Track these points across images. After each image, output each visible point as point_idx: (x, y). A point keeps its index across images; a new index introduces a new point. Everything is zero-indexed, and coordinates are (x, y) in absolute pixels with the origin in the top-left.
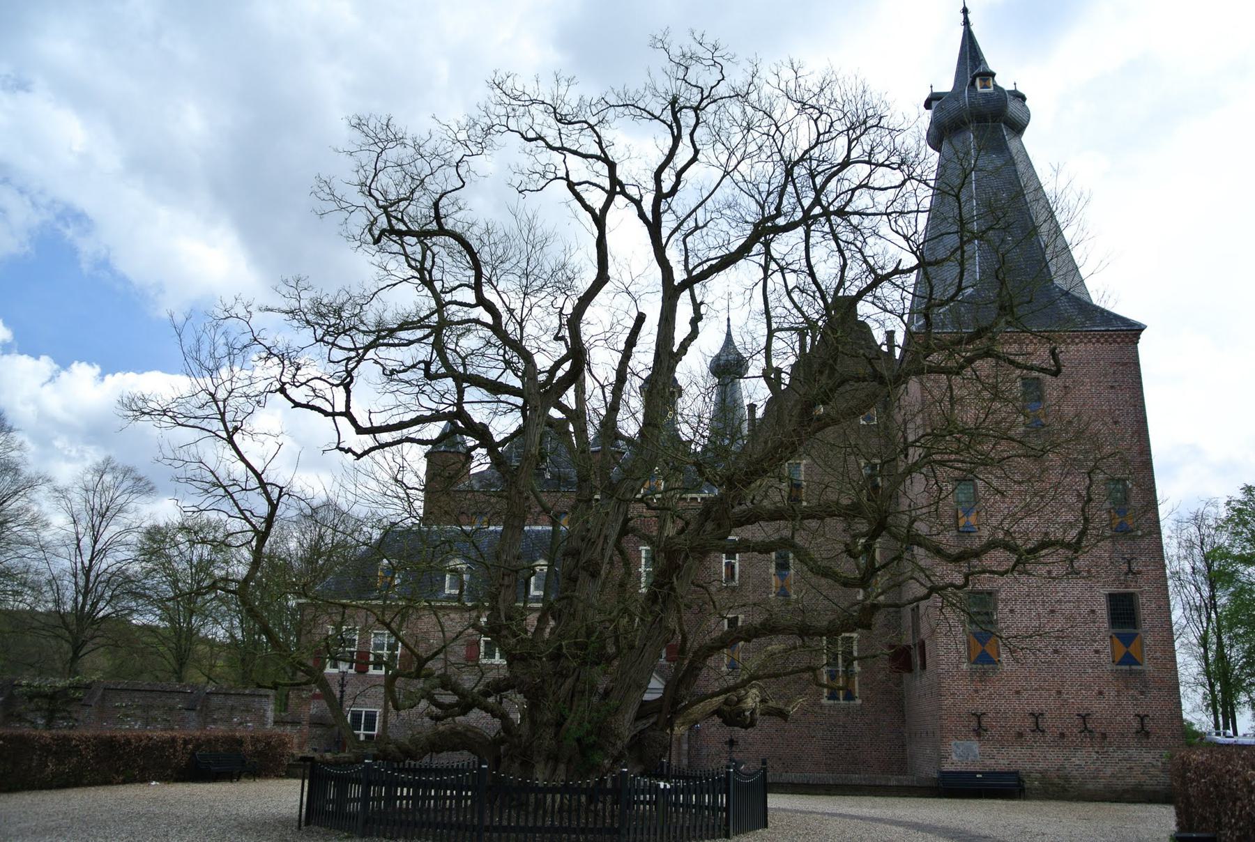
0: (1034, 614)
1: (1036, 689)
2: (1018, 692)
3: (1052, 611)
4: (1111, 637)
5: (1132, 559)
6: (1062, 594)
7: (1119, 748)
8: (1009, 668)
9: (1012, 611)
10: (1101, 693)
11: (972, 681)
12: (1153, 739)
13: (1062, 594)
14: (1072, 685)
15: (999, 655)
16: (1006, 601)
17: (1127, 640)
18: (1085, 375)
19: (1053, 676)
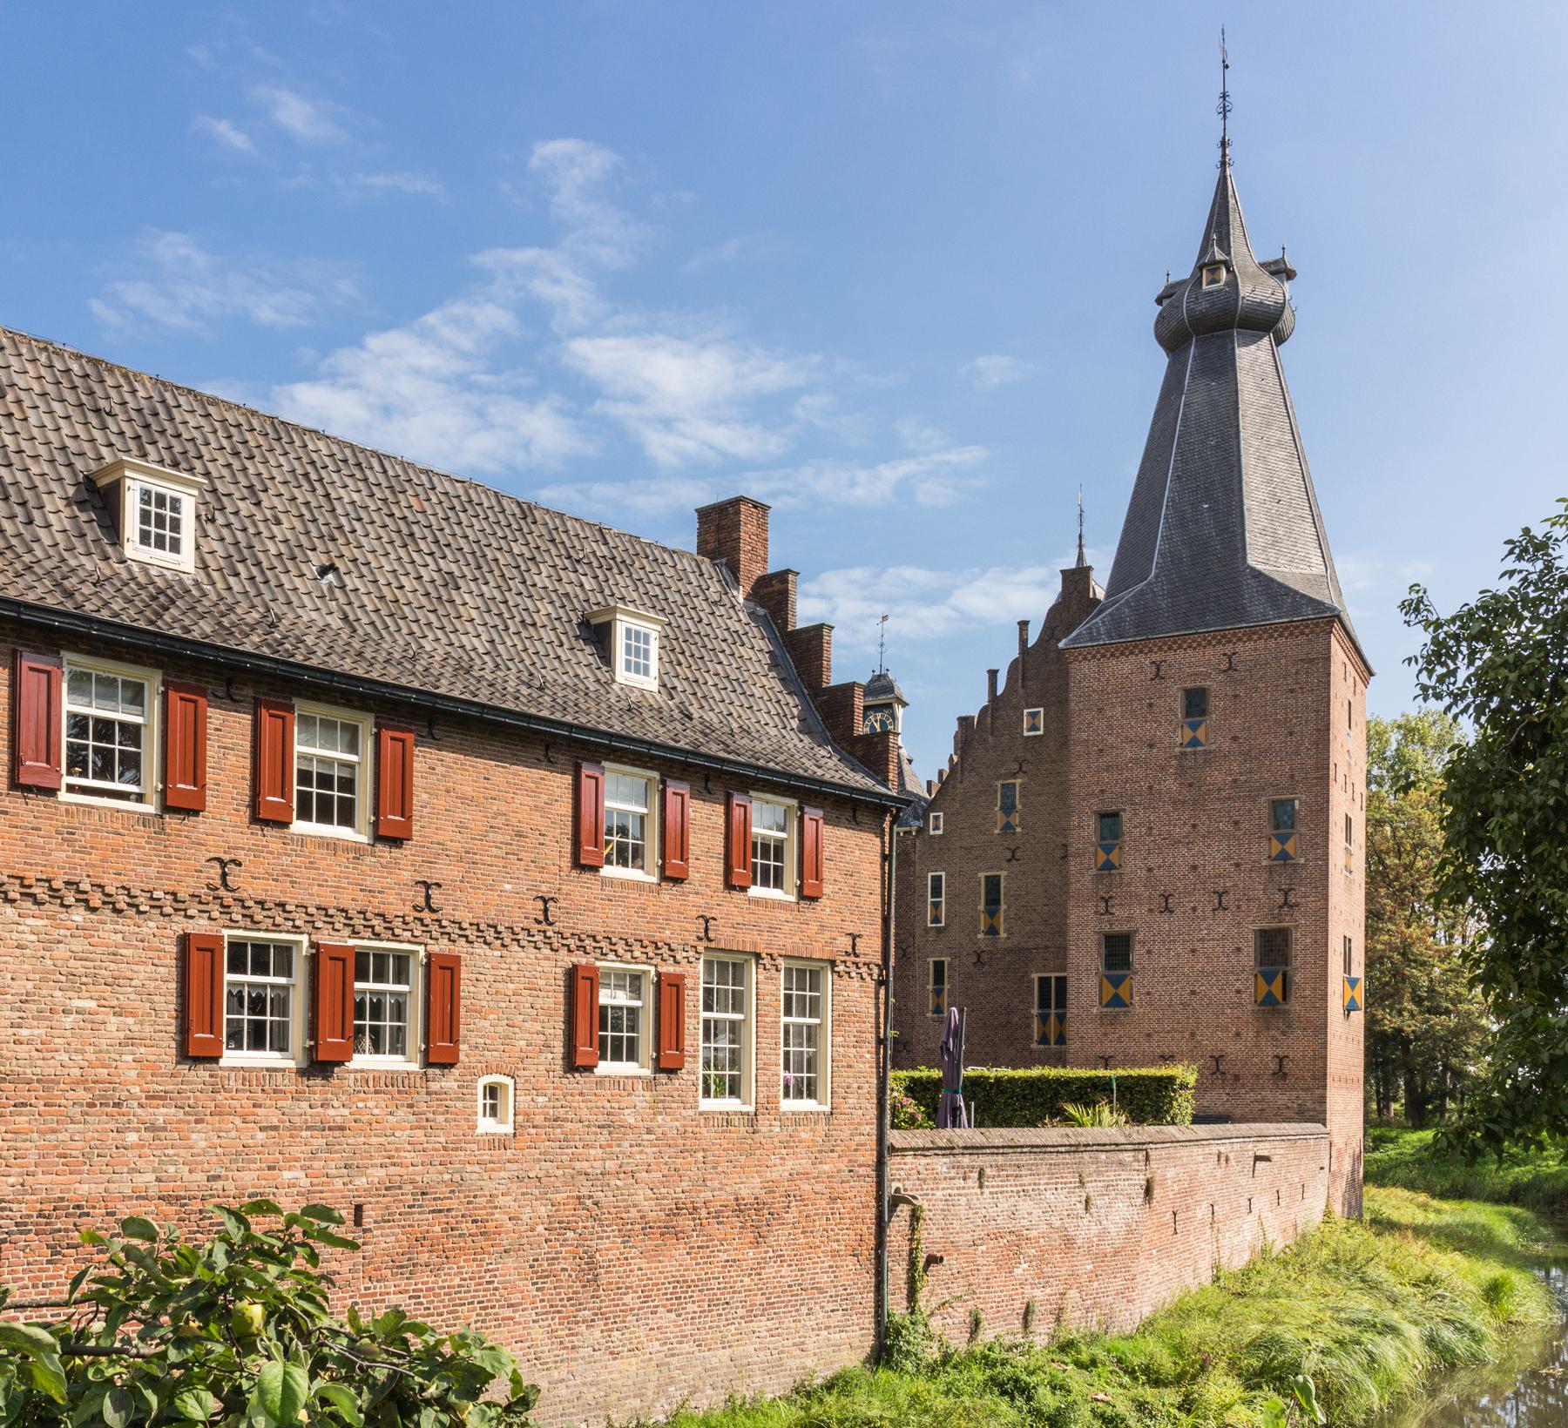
1: (1168, 1032)
2: (1148, 1035)
3: (1193, 951)
7: (1252, 1090)
9: (1149, 952)
10: (1238, 1034)
12: (1290, 1080)
15: (1132, 998)
16: (1143, 943)
17: (1116, 982)
18: (1261, 678)
19: (1188, 1018)
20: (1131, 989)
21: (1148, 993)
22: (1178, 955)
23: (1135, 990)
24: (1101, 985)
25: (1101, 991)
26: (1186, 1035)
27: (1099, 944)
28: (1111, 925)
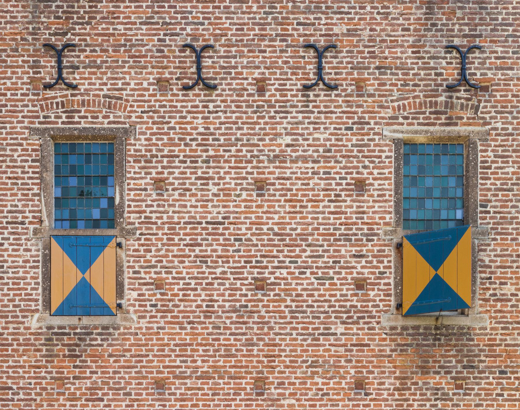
0: (214, 190)
1: (206, 376)
4: (399, 247)
5: (471, 49)
6: (288, 140)
8: (143, 323)
11: (50, 356)
13: (288, 140)
14: (292, 366)
19: (250, 343)
20: (119, 272)
21: (159, 285)
22: (227, 192)
23: (128, 274)
24: (47, 260)
25: (47, 277)
26: (246, 382)
27: (42, 160)
28: (70, 114)
